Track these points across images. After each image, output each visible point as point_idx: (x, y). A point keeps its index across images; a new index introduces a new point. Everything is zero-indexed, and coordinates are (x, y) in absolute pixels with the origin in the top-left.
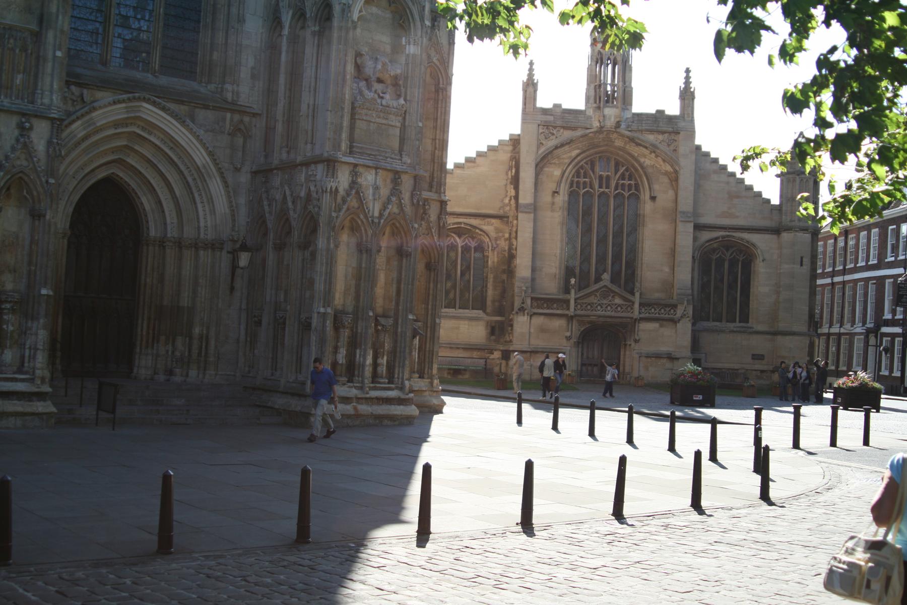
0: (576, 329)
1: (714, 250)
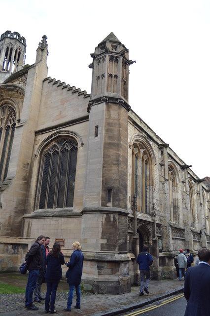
1: (54, 146)
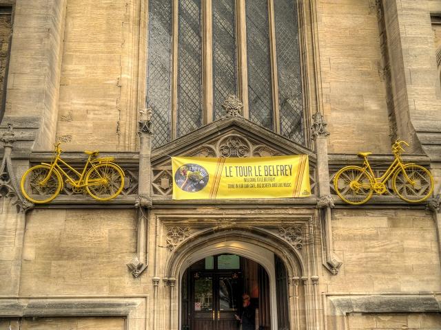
0: (159, 248)
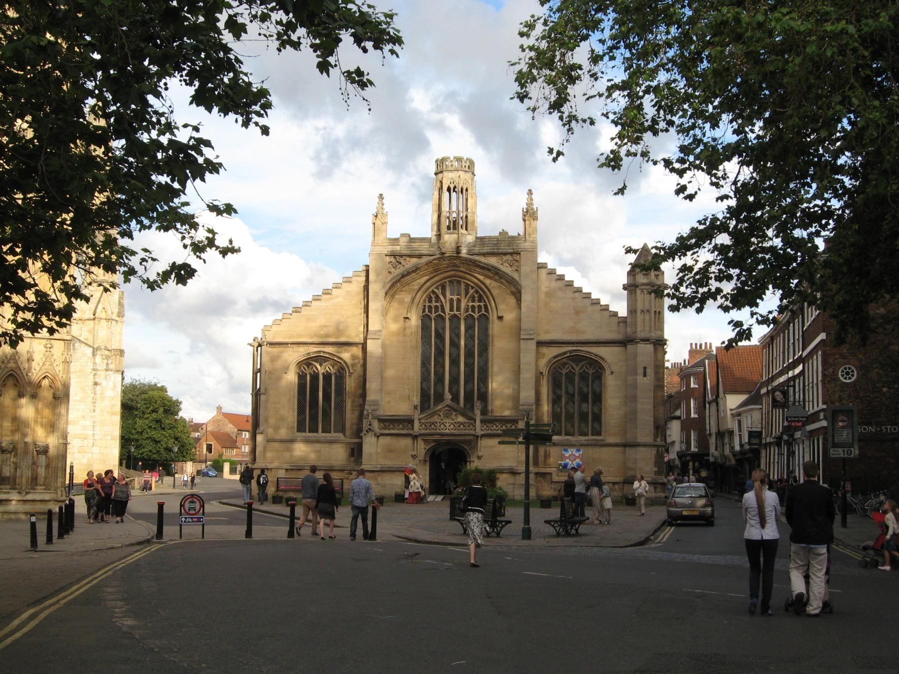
0: (422, 448)
1: (565, 364)
